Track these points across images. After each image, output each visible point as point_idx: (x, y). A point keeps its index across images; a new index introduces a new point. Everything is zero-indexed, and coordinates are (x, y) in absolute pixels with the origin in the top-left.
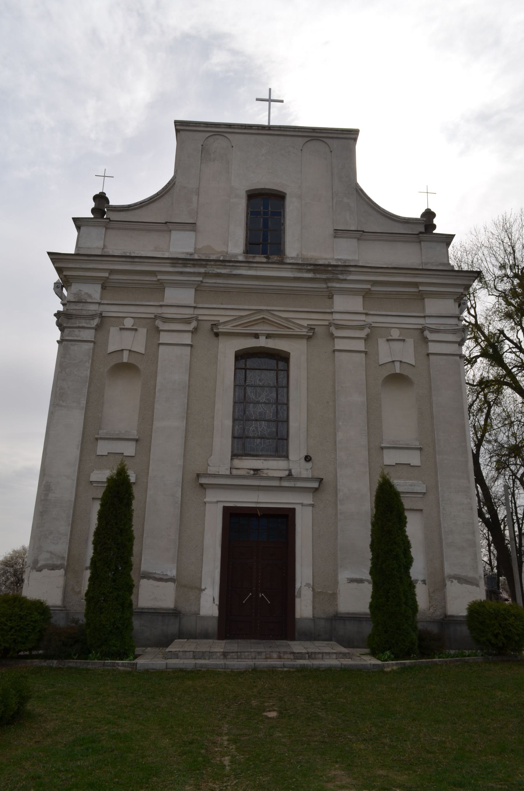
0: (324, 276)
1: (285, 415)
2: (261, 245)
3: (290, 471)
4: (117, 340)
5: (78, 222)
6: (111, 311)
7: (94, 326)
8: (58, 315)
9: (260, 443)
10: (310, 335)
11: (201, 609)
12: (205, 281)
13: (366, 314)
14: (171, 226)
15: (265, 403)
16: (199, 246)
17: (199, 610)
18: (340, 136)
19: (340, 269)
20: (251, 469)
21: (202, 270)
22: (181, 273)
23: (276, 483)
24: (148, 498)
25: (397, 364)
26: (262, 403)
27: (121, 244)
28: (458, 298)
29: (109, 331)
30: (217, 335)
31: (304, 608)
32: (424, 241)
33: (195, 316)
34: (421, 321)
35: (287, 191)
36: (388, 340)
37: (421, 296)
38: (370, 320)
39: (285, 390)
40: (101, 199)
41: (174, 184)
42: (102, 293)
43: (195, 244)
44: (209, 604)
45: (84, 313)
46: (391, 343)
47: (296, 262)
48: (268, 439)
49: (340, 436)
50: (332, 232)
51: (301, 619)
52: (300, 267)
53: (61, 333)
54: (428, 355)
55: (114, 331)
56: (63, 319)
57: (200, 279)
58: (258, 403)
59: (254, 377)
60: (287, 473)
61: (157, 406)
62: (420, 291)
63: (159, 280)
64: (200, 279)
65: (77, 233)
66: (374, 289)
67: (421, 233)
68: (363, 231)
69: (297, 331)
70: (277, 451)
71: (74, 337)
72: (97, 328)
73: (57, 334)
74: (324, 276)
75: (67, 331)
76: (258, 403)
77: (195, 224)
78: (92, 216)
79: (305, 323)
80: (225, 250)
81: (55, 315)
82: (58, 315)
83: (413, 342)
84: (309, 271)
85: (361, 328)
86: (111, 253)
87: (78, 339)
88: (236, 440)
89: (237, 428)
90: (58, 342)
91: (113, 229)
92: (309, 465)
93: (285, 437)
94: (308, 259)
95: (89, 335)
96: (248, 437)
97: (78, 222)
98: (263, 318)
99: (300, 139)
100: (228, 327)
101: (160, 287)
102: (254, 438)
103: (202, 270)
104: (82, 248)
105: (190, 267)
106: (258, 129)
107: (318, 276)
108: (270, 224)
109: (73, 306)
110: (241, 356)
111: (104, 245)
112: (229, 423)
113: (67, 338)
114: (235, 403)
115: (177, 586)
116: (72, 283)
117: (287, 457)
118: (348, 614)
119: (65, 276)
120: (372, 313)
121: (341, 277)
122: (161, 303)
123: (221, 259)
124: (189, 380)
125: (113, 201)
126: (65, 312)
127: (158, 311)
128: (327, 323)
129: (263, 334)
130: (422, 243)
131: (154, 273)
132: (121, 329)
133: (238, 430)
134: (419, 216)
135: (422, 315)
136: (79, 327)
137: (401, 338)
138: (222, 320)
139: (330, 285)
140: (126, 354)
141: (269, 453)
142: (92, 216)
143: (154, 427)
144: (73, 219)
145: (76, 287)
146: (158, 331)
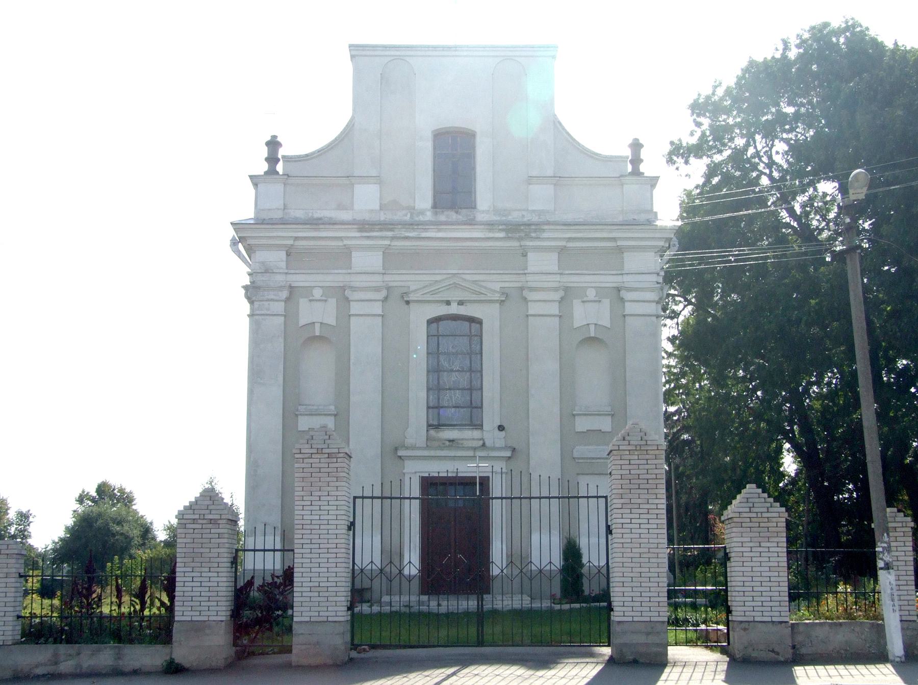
0: (517, 235)
1: (479, 383)
3: (482, 439)
6: (300, 280)
8: (246, 288)
10: (505, 298)
13: (561, 274)
15: (458, 371)
19: (533, 227)
21: (390, 234)
22: (368, 237)
23: (471, 453)
29: (298, 303)
30: (408, 302)
34: (619, 279)
35: (478, 130)
36: (583, 302)
37: (620, 250)
38: (565, 279)
39: (479, 356)
40: (273, 144)
43: (381, 199)
46: (586, 304)
54: (624, 316)
55: (303, 303)
56: (252, 292)
57: (387, 242)
58: (452, 371)
59: (446, 345)
60: (481, 443)
64: (387, 242)
65: (253, 191)
66: (570, 245)
69: (490, 296)
72: (287, 300)
73: (246, 307)
74: (517, 235)
75: (256, 304)
76: (452, 371)
79: (497, 286)
82: (246, 288)
88: (430, 410)
92: (503, 433)
101: (347, 253)
112: (423, 394)
113: (258, 312)
114: (428, 372)
117: (480, 427)
120: (567, 272)
121: (533, 235)
122: (349, 271)
129: (455, 301)
131: (340, 239)
132: (310, 301)
136: (268, 300)
137: (597, 299)
139: (523, 243)
140: (317, 326)
144: (251, 177)
145: (261, 256)
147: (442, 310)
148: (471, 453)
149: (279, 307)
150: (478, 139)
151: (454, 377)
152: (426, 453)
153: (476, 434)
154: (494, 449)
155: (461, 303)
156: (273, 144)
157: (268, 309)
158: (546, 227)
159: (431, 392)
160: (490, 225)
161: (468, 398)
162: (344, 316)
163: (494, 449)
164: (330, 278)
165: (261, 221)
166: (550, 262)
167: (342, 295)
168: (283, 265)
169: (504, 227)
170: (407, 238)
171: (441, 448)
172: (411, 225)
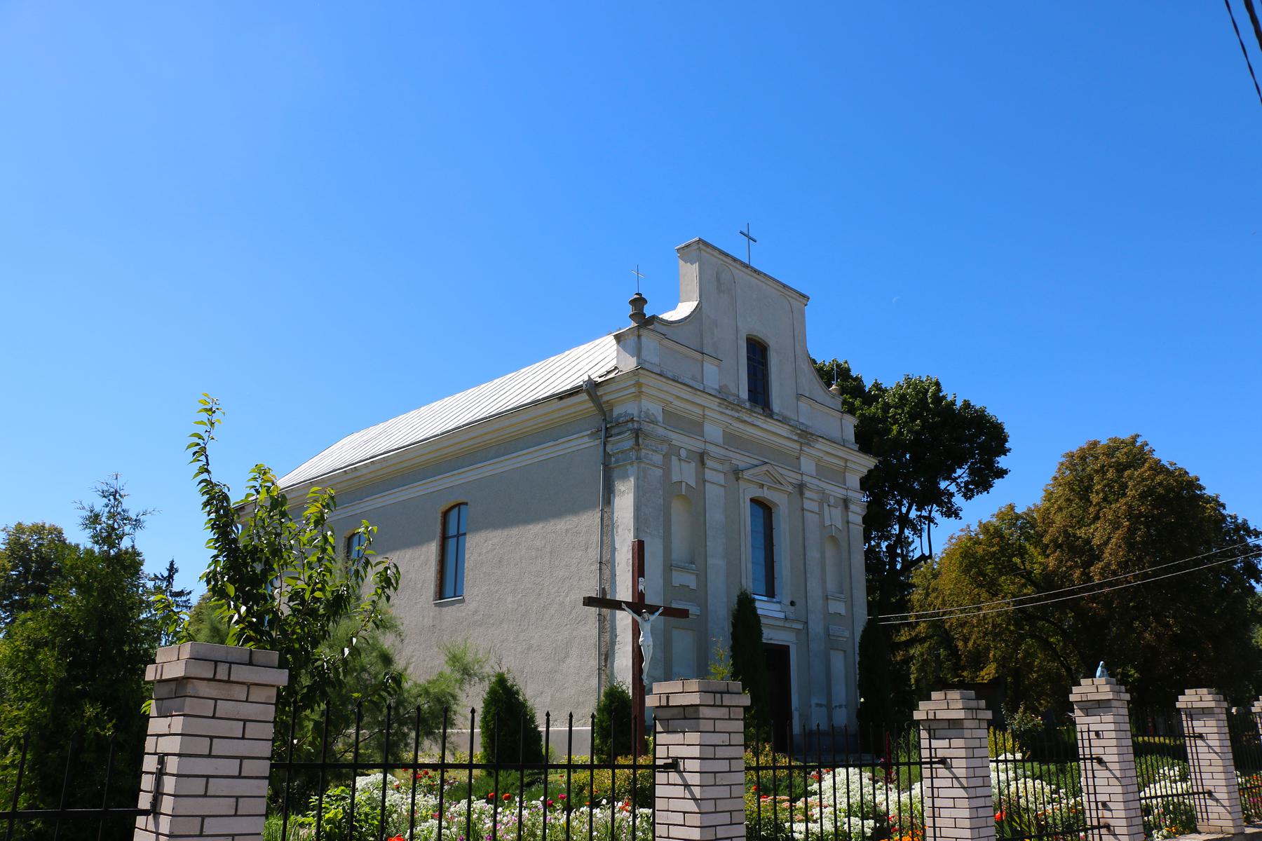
6: (677, 439)
21: (736, 415)
23: (781, 624)
30: (738, 479)
40: (639, 302)
95: (658, 458)
103: (736, 415)
156: (639, 302)
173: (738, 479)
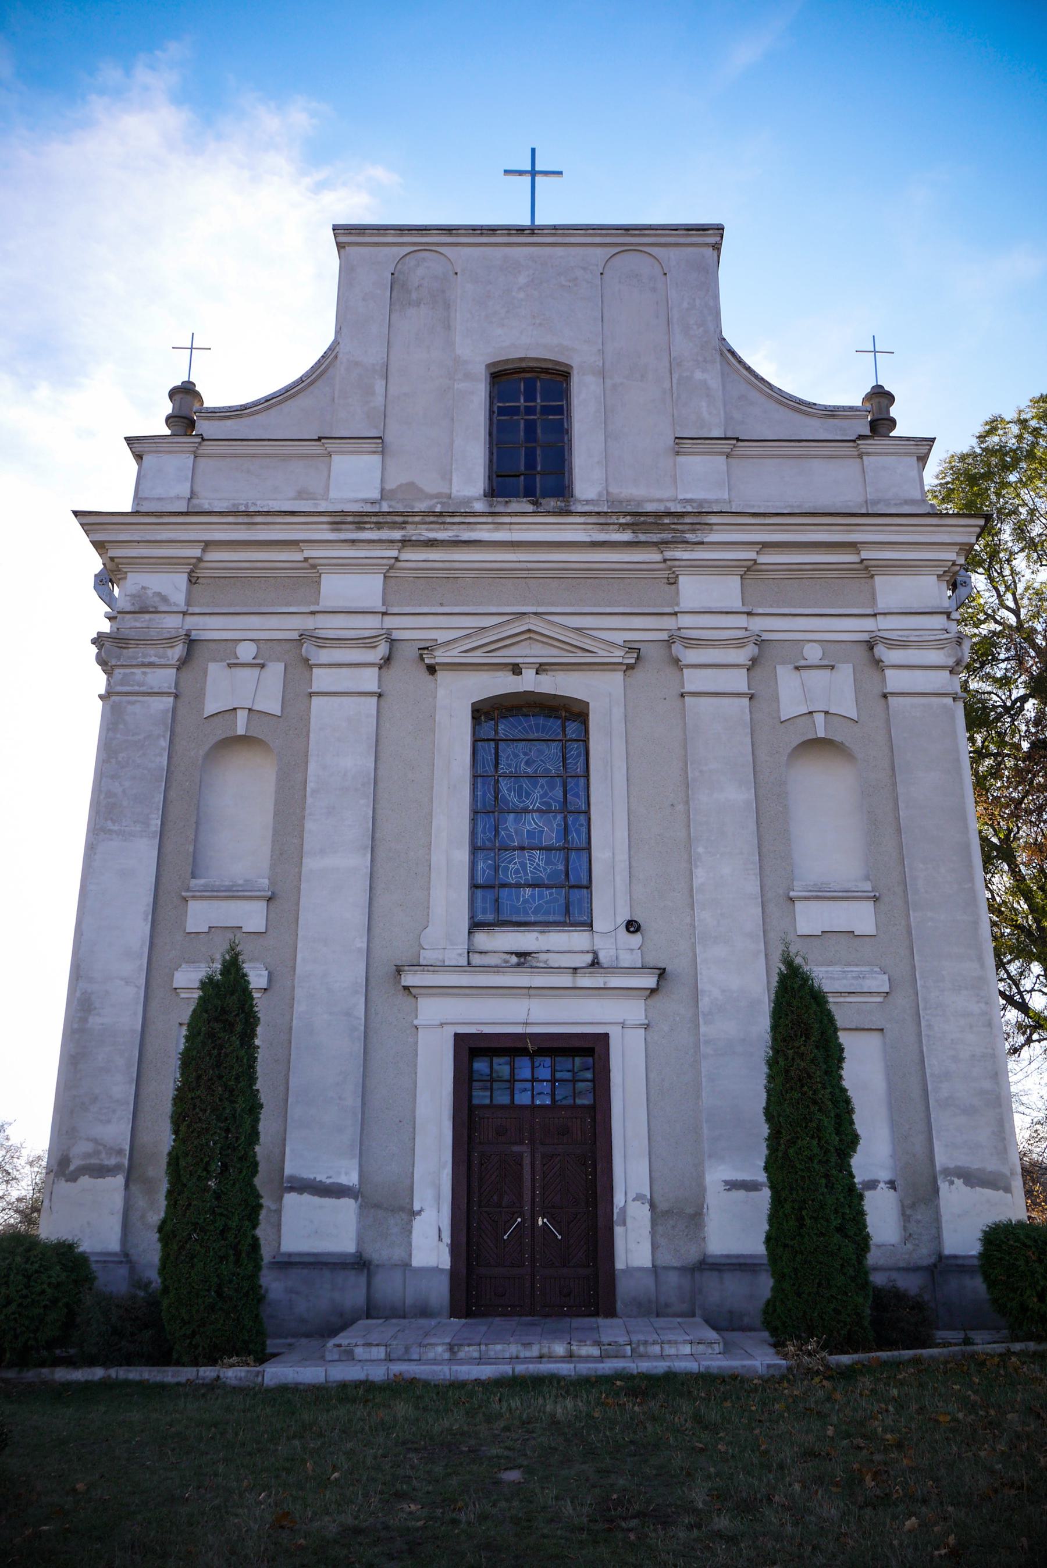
1: (584, 836)
2: (522, 478)
3: (595, 954)
4: (224, 689)
5: (138, 446)
6: (211, 628)
7: (173, 662)
8: (99, 640)
9: (532, 896)
11: (414, 1253)
12: (404, 556)
13: (749, 614)
14: (331, 446)
16: (390, 486)
17: (410, 1255)
18: (682, 240)
19: (687, 520)
20: (512, 953)
21: (397, 535)
23: (566, 980)
24: (295, 1022)
25: (820, 718)
26: (533, 811)
27: (224, 487)
28: (945, 572)
30: (432, 669)
31: (634, 1247)
32: (868, 454)
33: (384, 631)
34: (869, 624)
35: (575, 362)
37: (867, 570)
38: (757, 624)
39: (582, 781)
41: (336, 357)
42: (189, 593)
44: (429, 1244)
45: (153, 633)
46: (805, 673)
47: (596, 510)
48: (548, 887)
49: (700, 875)
50: (671, 441)
51: (629, 1271)
52: (602, 520)
53: (108, 680)
54: (885, 696)
55: (215, 671)
56: (110, 649)
57: (394, 553)
58: (526, 810)
60: (589, 958)
61: (309, 825)
62: (862, 560)
63: (306, 559)
65: (136, 467)
66: (763, 559)
67: (861, 437)
68: (738, 440)
69: (603, 655)
70: (568, 912)
71: (132, 686)
73: (99, 681)
74: (655, 538)
77: (380, 438)
78: (168, 432)
79: (619, 638)
80: (448, 491)
81: (94, 642)
82: (99, 640)
83: (851, 670)
84: (623, 527)
85: (739, 643)
86: (207, 507)
87: (144, 689)
88: (479, 893)
89: (481, 865)
90: (101, 697)
91: (209, 456)
92: (636, 939)
93: (585, 882)
94: (621, 502)
96: (504, 885)
97: (138, 446)
98: (529, 631)
99: (599, 251)
100: (455, 652)
101: (311, 574)
102: (518, 886)
103: (397, 535)
104: (146, 499)
105: (371, 528)
106: (509, 235)
107: (642, 537)
108: (539, 431)
109: (130, 621)
110: (485, 713)
111: (192, 492)
112: (462, 855)
113: (119, 689)
114: (475, 813)
115: (361, 1207)
116: (126, 573)
118: (728, 1256)
119: (112, 559)
120: (760, 611)
121: (690, 537)
123: (437, 510)
124: (376, 769)
125: (211, 400)
126: (113, 635)
127: (309, 623)
128: (664, 636)
130: (864, 458)
131: (294, 543)
133: (484, 871)
134: (858, 403)
135: (869, 611)
136: (143, 665)
137: (825, 662)
138: (442, 637)
139: (669, 554)
140: (242, 716)
141: (551, 918)
142: (168, 432)
143: (304, 869)
144: (127, 439)
145: (135, 580)
146: (308, 665)
147: (503, 684)
148: (566, 980)
149: (164, 678)
150: (575, 379)
151: (532, 822)
152: (464, 980)
153: (578, 939)
154: (616, 969)
155: (541, 669)
157: (140, 685)
158: (714, 520)
159: (481, 855)
160: (602, 517)
161: (561, 867)
162: (299, 694)
163: (616, 969)
164: (273, 622)
165: (135, 513)
166: (727, 591)
167: (298, 654)
168: (179, 598)
169: (628, 519)
170: (431, 543)
171: (496, 969)
172: (439, 517)
173: (432, 669)
